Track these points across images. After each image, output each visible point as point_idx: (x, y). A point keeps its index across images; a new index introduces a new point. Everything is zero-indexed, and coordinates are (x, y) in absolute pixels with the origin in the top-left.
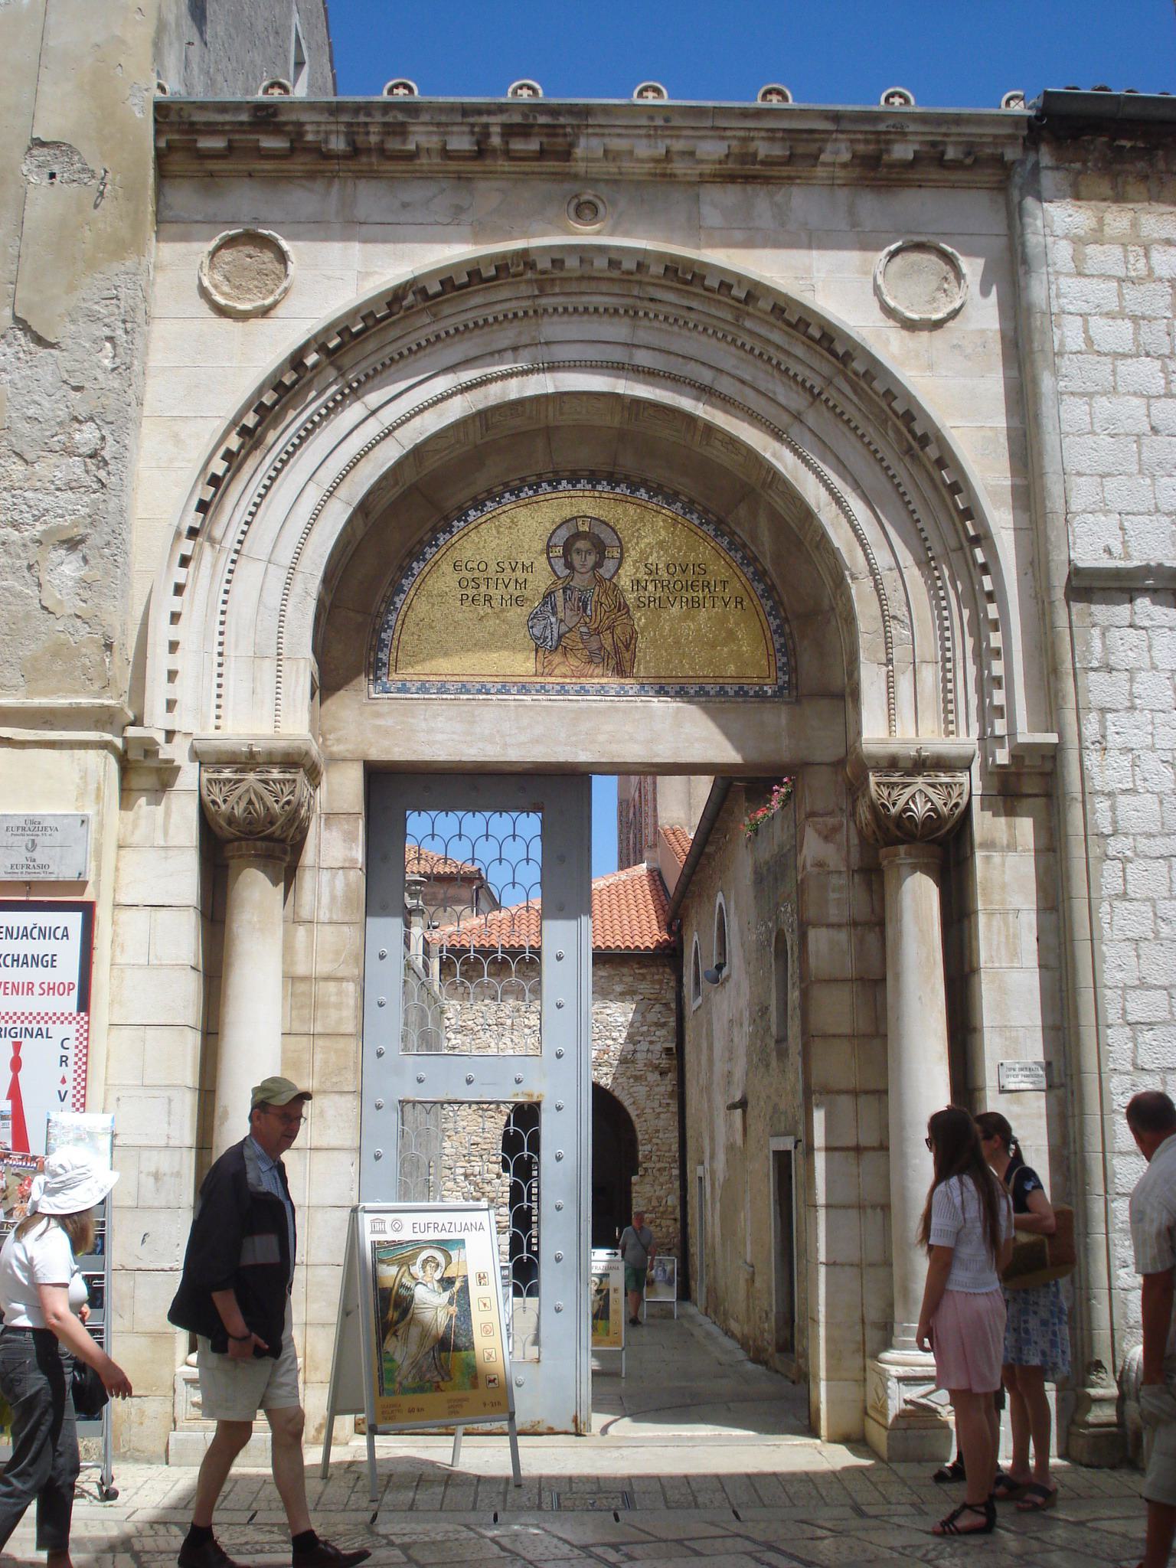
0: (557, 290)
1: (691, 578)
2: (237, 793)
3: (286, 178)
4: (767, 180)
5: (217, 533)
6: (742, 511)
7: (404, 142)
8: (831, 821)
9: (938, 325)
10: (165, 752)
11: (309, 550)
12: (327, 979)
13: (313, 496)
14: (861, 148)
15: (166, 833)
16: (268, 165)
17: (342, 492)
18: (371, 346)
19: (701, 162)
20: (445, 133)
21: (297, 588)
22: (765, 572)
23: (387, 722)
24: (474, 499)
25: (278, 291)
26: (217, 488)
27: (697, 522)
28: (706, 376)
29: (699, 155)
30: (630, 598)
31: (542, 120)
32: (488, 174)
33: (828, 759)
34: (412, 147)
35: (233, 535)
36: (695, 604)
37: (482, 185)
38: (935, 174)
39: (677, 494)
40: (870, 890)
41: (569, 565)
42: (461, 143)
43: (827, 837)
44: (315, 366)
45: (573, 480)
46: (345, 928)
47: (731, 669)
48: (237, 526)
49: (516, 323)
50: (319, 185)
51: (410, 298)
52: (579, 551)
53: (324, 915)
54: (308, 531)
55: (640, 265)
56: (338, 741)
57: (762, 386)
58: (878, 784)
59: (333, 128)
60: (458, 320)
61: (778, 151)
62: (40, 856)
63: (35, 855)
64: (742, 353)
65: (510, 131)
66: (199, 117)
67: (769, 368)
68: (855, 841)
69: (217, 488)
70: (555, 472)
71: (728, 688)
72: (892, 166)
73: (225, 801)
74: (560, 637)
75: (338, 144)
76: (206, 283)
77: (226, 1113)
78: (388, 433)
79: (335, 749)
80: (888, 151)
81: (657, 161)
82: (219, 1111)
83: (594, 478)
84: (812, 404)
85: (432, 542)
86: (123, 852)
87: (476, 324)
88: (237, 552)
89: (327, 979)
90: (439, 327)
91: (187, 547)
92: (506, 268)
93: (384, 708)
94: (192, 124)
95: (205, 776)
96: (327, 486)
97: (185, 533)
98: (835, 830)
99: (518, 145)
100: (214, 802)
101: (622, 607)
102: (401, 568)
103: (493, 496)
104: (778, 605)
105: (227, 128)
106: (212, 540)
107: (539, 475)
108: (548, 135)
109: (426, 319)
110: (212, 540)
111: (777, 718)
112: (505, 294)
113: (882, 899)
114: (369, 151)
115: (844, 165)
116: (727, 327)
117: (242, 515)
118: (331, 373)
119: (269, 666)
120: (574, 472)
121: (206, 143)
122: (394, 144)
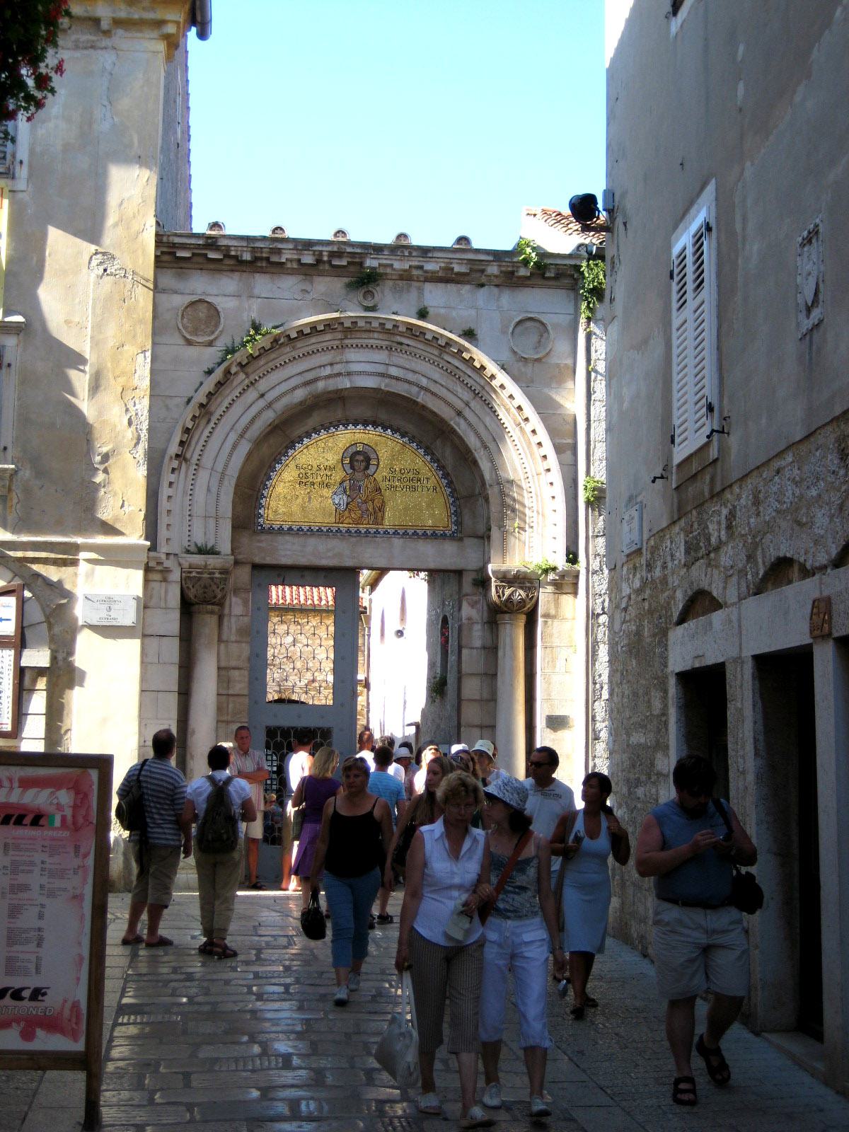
0: (353, 336)
1: (411, 475)
2: (199, 583)
3: (220, 271)
4: (458, 282)
5: (188, 456)
6: (438, 442)
7: (280, 258)
8: (475, 598)
9: (538, 360)
10: (168, 564)
11: (231, 464)
12: (234, 668)
13: (233, 437)
14: (503, 269)
15: (166, 600)
16: (212, 266)
17: (247, 436)
18: (262, 362)
19: (426, 272)
20: (301, 254)
21: (226, 482)
22: (448, 474)
23: (263, 545)
24: (307, 432)
25: (217, 333)
26: (189, 434)
27: (416, 447)
28: (424, 382)
29: (425, 268)
30: (383, 485)
31: (349, 250)
32: (321, 274)
33: (475, 568)
34: (284, 261)
35: (196, 457)
36: (415, 489)
37: (317, 279)
38: (541, 282)
39: (406, 433)
40: (492, 632)
41: (352, 467)
42: (308, 259)
43: (473, 605)
44: (235, 374)
45: (355, 424)
46: (244, 645)
47: (430, 522)
48: (198, 452)
49: (333, 351)
50: (236, 275)
51: (282, 340)
52: (357, 461)
53: (233, 638)
54: (231, 455)
55: (394, 326)
56: (240, 554)
57: (450, 387)
58: (496, 586)
59: (245, 249)
60: (305, 350)
61: (464, 269)
62: (113, 614)
63: (110, 613)
64: (441, 371)
65: (333, 255)
66: (177, 240)
67: (455, 379)
68: (485, 608)
69: (189, 434)
70: (347, 420)
71: (428, 532)
72: (519, 278)
73: (193, 587)
74: (348, 504)
75: (247, 257)
76: (181, 327)
77: (194, 732)
78: (269, 405)
79: (240, 557)
80: (517, 271)
81: (405, 271)
82: (190, 730)
83: (365, 424)
84: (474, 398)
85: (285, 454)
86: (148, 610)
87: (313, 352)
88: (197, 465)
89: (234, 668)
90: (295, 354)
91: (175, 464)
92: (329, 326)
93: (263, 537)
94: (174, 244)
95: (184, 574)
96: (239, 432)
97: (174, 456)
98: (476, 602)
99: (336, 262)
100: (188, 588)
101: (378, 490)
102: (270, 467)
103: (317, 431)
104: (454, 491)
105: (192, 246)
106: (186, 460)
107: (339, 421)
108: (351, 257)
109: (288, 349)
110: (186, 460)
111: (450, 548)
112: (328, 337)
113: (497, 636)
114: (261, 259)
115: (496, 276)
116: (435, 358)
117: (199, 447)
118: (242, 376)
119: (212, 522)
120: (356, 420)
121: (180, 254)
122: (274, 259)
